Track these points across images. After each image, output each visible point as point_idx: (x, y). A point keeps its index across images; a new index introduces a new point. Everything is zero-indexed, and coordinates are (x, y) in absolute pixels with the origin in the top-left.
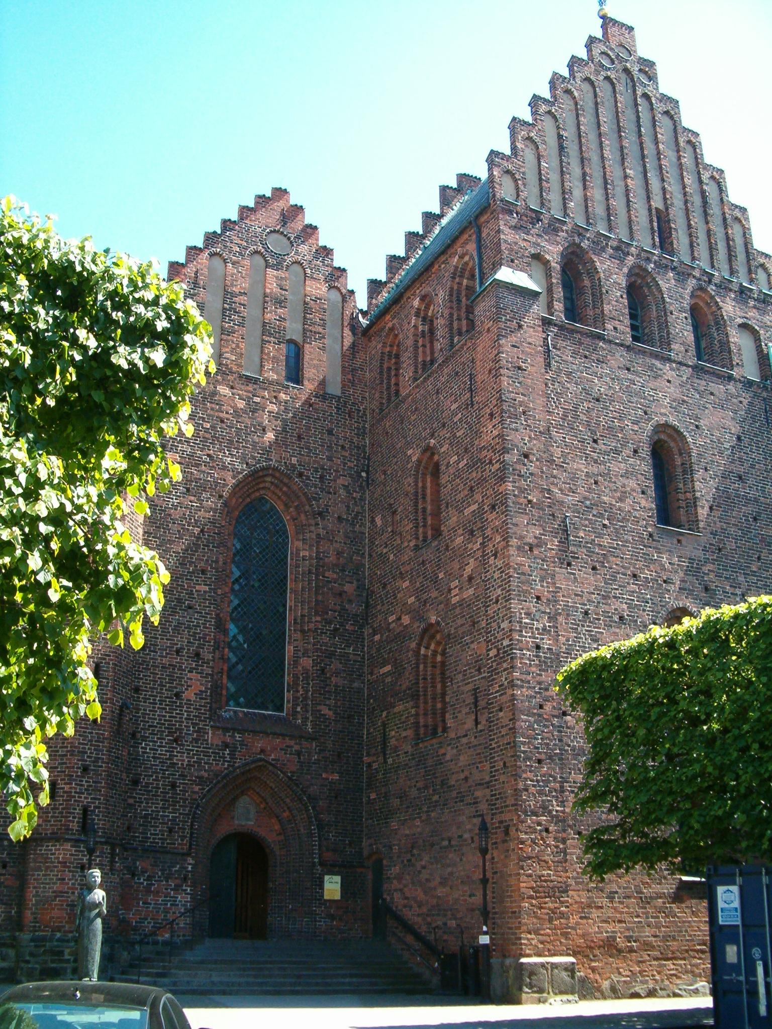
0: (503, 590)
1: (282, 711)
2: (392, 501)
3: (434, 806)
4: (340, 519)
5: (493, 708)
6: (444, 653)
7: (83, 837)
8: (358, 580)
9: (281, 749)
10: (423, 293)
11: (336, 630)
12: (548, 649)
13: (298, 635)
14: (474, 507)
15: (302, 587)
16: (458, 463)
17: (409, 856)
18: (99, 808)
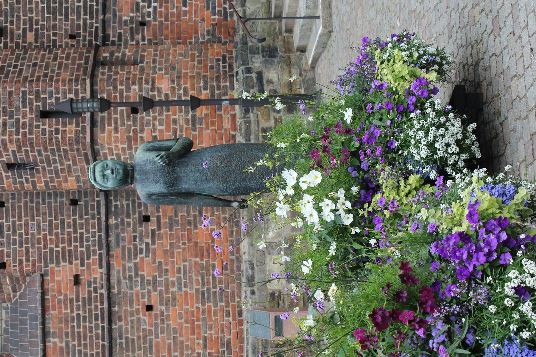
7: (88, 115)
18: (38, 93)
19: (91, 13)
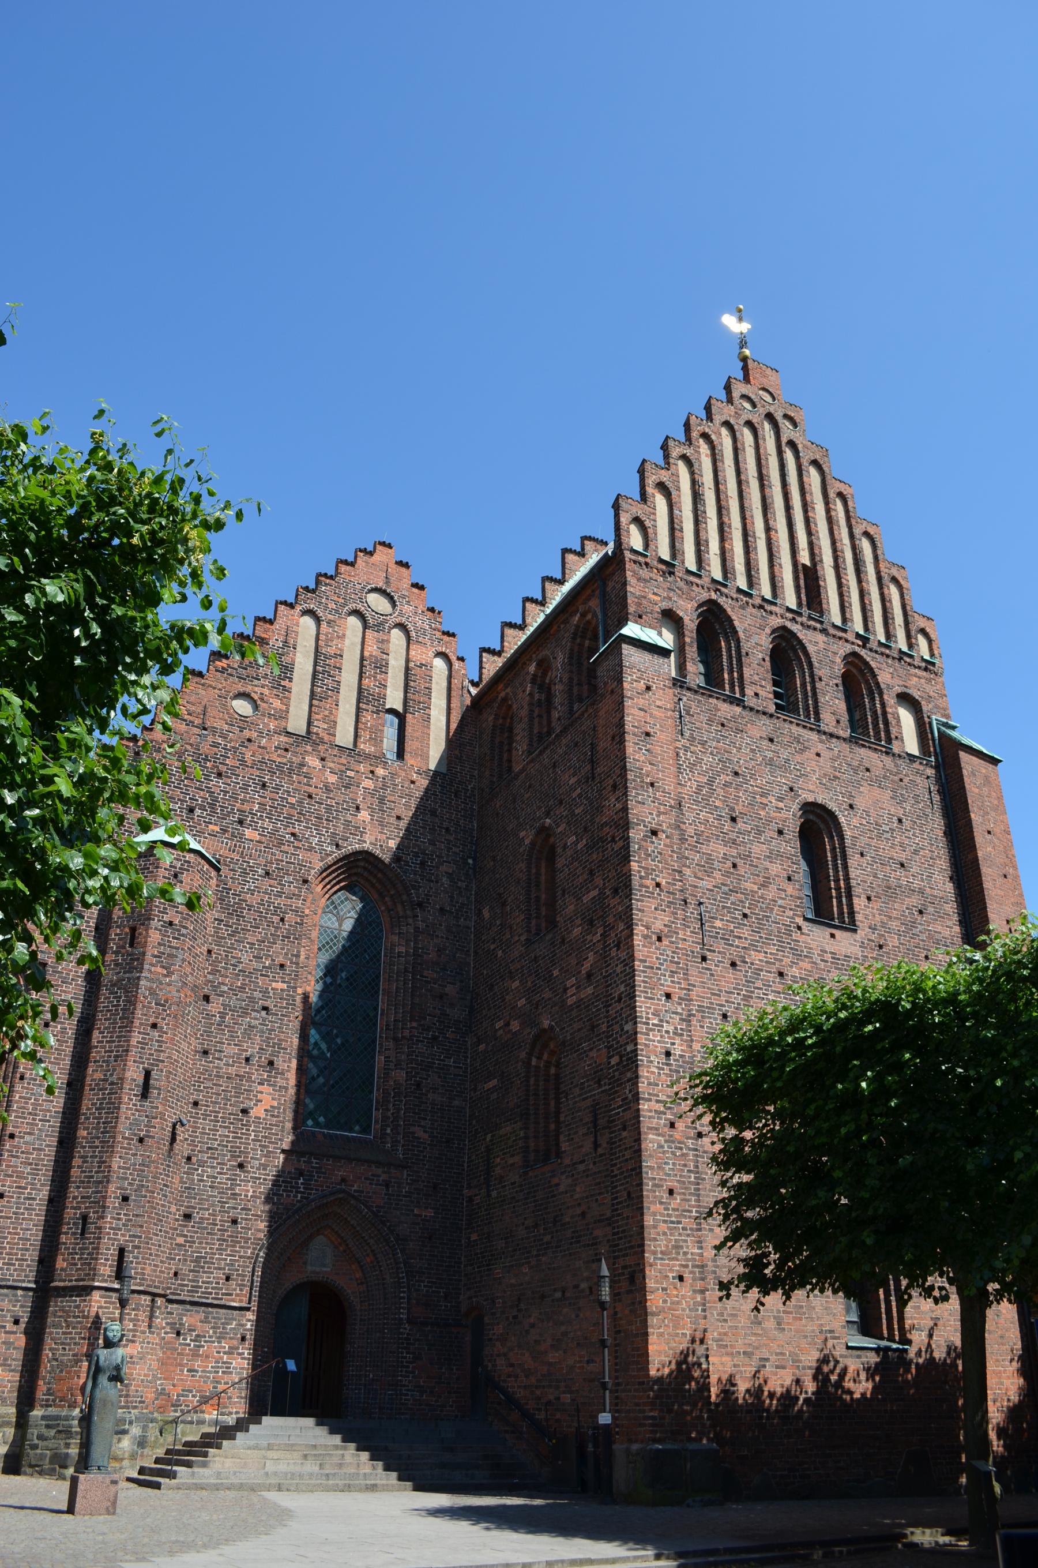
0: (626, 986)
2: (502, 890)
3: (545, 1249)
4: (442, 909)
5: (616, 1126)
6: (558, 1065)
7: (117, 1286)
8: (462, 981)
9: (366, 1179)
10: (540, 657)
11: (435, 1038)
12: (681, 1056)
13: (391, 1044)
14: (594, 893)
15: (397, 988)
16: (576, 843)
18: (139, 1247)
19: (192, 1291)
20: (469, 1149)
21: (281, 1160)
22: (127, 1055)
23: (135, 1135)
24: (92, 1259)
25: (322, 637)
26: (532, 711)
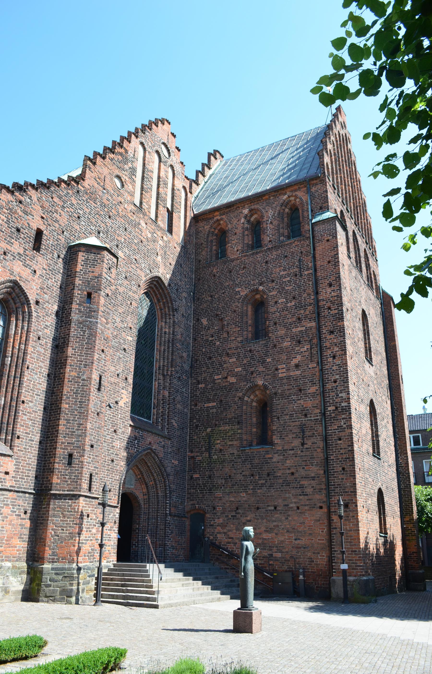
1: (150, 420)
4: (183, 314)
10: (253, 207)
11: (179, 377)
13: (161, 377)
15: (164, 349)
17: (234, 514)
20: (190, 433)
21: (130, 430)
22: (92, 365)
23: (96, 411)
24: (78, 479)
25: (146, 159)
26: (244, 232)
